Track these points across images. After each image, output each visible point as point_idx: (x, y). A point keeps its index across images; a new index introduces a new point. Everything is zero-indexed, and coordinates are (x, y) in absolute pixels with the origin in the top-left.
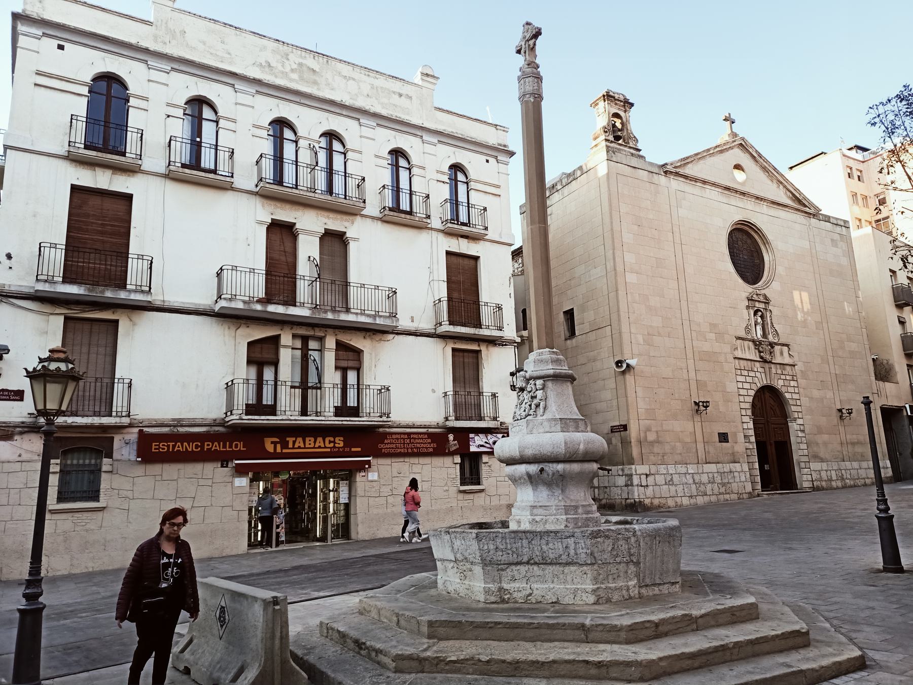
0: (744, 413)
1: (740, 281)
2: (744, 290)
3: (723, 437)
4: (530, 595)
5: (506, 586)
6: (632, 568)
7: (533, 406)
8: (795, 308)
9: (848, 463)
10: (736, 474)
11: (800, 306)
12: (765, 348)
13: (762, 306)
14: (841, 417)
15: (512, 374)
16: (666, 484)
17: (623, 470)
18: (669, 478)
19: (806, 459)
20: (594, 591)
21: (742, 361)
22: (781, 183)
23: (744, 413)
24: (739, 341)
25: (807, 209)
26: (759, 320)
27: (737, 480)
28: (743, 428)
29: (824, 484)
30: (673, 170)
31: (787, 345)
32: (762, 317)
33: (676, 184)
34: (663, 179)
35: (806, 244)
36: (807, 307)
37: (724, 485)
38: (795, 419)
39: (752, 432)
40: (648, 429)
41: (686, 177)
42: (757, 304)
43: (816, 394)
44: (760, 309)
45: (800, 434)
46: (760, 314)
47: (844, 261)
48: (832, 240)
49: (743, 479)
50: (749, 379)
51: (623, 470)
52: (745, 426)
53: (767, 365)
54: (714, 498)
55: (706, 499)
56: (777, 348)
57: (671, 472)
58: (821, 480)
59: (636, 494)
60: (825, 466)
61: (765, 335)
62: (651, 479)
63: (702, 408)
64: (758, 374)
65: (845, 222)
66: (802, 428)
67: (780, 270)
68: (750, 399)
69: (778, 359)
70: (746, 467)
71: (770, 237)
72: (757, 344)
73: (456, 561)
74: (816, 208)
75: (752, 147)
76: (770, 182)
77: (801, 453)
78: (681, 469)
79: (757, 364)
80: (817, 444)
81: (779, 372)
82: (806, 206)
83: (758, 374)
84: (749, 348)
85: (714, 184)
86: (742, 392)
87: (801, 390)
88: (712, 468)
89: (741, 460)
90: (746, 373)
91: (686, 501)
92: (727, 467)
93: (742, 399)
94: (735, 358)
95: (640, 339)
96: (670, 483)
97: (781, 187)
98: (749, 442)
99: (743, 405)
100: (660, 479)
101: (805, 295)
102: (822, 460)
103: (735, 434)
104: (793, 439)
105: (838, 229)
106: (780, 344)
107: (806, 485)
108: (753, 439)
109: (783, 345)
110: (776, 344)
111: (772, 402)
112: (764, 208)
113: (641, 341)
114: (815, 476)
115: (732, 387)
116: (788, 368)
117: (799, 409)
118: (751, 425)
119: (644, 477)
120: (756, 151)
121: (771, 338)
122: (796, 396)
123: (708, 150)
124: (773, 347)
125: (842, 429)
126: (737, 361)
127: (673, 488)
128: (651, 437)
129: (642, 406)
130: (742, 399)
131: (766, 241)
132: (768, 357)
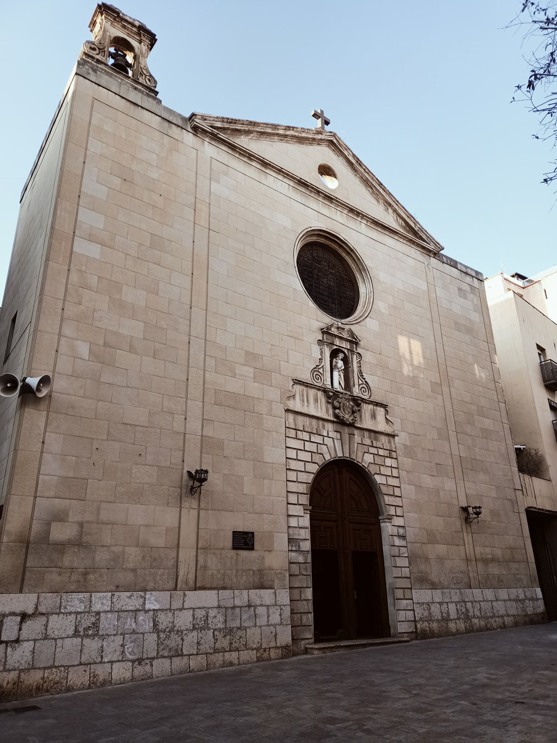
0: (293, 499)
1: (311, 304)
2: (315, 318)
3: (244, 541)
8: (399, 358)
9: (477, 592)
10: (261, 611)
11: (407, 356)
12: (346, 408)
13: (345, 345)
16: (76, 633)
18: (87, 621)
19: (406, 583)
21: (300, 418)
22: (390, 205)
23: (293, 499)
24: (298, 388)
25: (425, 244)
26: (340, 364)
27: (262, 621)
28: (286, 523)
29: (435, 625)
30: (209, 129)
31: (384, 406)
32: (346, 360)
33: (210, 150)
34: (189, 138)
35: (424, 286)
36: (418, 359)
37: (228, 632)
38: (390, 518)
39: (306, 534)
40: (60, 517)
41: (233, 147)
42: (337, 342)
43: (428, 481)
44: (342, 351)
45: (397, 542)
46: (341, 356)
47: (476, 317)
48: (460, 289)
49: (275, 618)
50: (313, 447)
52: (293, 522)
53: (346, 430)
54: (196, 663)
55: (178, 663)
56: (367, 409)
57: (97, 607)
58: (430, 619)
60: (437, 595)
61: (348, 385)
62: (33, 628)
64: (328, 441)
65: (477, 273)
66: (401, 531)
67: (381, 306)
68: (310, 478)
69: (367, 423)
70: (284, 597)
71: (368, 262)
72: (331, 396)
74: (436, 244)
75: (348, 149)
76: (375, 202)
77: (397, 572)
78: (127, 601)
79: (330, 426)
80: (427, 559)
81: (367, 441)
83: (328, 441)
84: (316, 400)
85: (280, 171)
86: (293, 465)
87: (403, 474)
88: (209, 598)
89: (276, 583)
90: (306, 436)
91: (121, 672)
92: (242, 597)
93: (292, 476)
94: (288, 411)
95: (84, 349)
96: (93, 631)
97: (390, 211)
98: (299, 551)
99: (293, 487)
100: (61, 625)
101: (416, 345)
102: (434, 586)
103: (270, 536)
104: (386, 549)
105: (468, 279)
106: (371, 403)
107: (403, 628)
108: (307, 546)
109: (377, 404)
110: (363, 400)
112: (362, 227)
113: (86, 355)
114: (420, 612)
115: (275, 455)
116: (383, 439)
117: (398, 501)
118: (306, 521)
120: (354, 156)
121: (356, 391)
122: (392, 481)
123: (275, 127)
124: (359, 405)
125: (468, 538)
126: (291, 416)
127: (92, 645)
128: (60, 533)
129: (52, 469)
130: (292, 476)
131: (362, 268)
132: (348, 417)
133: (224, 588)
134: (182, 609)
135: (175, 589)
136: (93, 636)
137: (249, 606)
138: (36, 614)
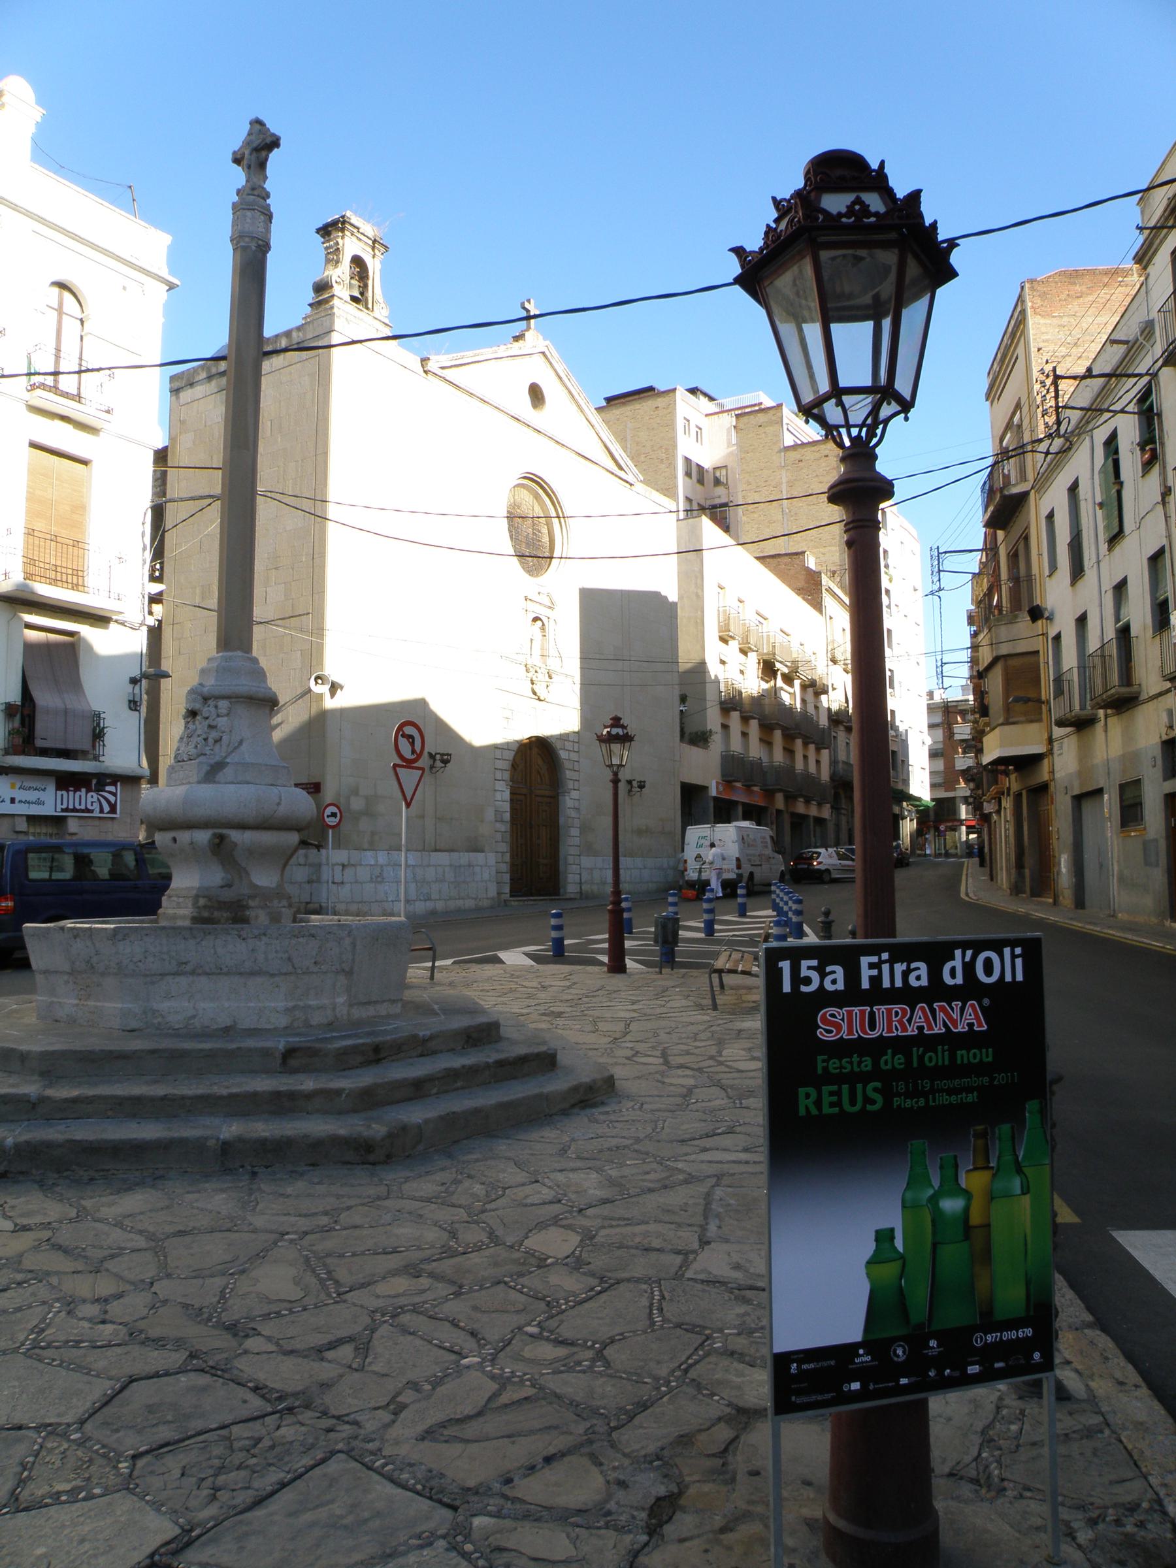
0: (499, 775)
4: (194, 1017)
5: (155, 1006)
6: (342, 980)
7: (211, 741)
10: (477, 869)
14: (630, 791)
15: (134, 681)
17: (306, 856)
18: (377, 871)
20: (288, 1010)
29: (595, 888)
46: (539, 623)
49: (486, 876)
51: (306, 856)
54: (440, 906)
55: (430, 905)
59: (324, 895)
62: (349, 872)
63: (439, 764)
66: (577, 804)
73: (73, 973)
82: (621, 468)
88: (443, 858)
92: (464, 858)
100: (363, 873)
108: (507, 816)
111: (540, 762)
117: (574, 775)
118: (507, 795)
119: (338, 869)
122: (574, 756)
133: (452, 850)
134: (429, 866)
135: (424, 850)
136: (380, 882)
137: (469, 866)
138: (350, 865)
